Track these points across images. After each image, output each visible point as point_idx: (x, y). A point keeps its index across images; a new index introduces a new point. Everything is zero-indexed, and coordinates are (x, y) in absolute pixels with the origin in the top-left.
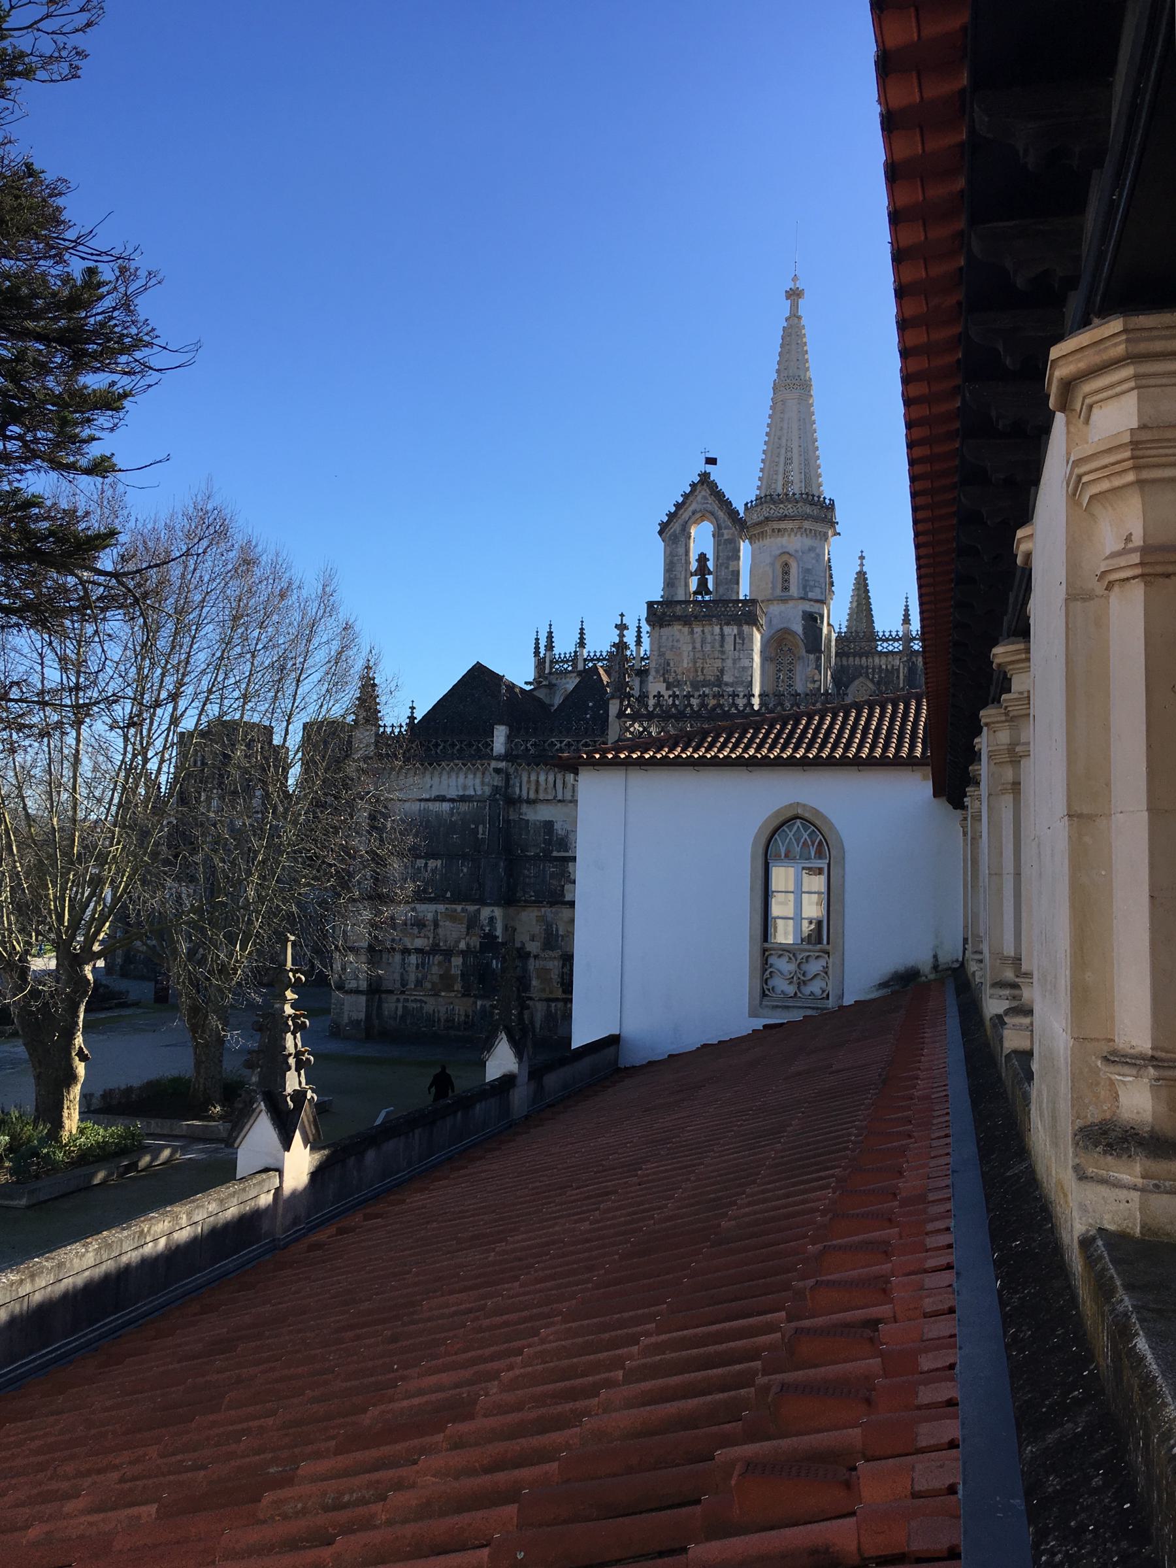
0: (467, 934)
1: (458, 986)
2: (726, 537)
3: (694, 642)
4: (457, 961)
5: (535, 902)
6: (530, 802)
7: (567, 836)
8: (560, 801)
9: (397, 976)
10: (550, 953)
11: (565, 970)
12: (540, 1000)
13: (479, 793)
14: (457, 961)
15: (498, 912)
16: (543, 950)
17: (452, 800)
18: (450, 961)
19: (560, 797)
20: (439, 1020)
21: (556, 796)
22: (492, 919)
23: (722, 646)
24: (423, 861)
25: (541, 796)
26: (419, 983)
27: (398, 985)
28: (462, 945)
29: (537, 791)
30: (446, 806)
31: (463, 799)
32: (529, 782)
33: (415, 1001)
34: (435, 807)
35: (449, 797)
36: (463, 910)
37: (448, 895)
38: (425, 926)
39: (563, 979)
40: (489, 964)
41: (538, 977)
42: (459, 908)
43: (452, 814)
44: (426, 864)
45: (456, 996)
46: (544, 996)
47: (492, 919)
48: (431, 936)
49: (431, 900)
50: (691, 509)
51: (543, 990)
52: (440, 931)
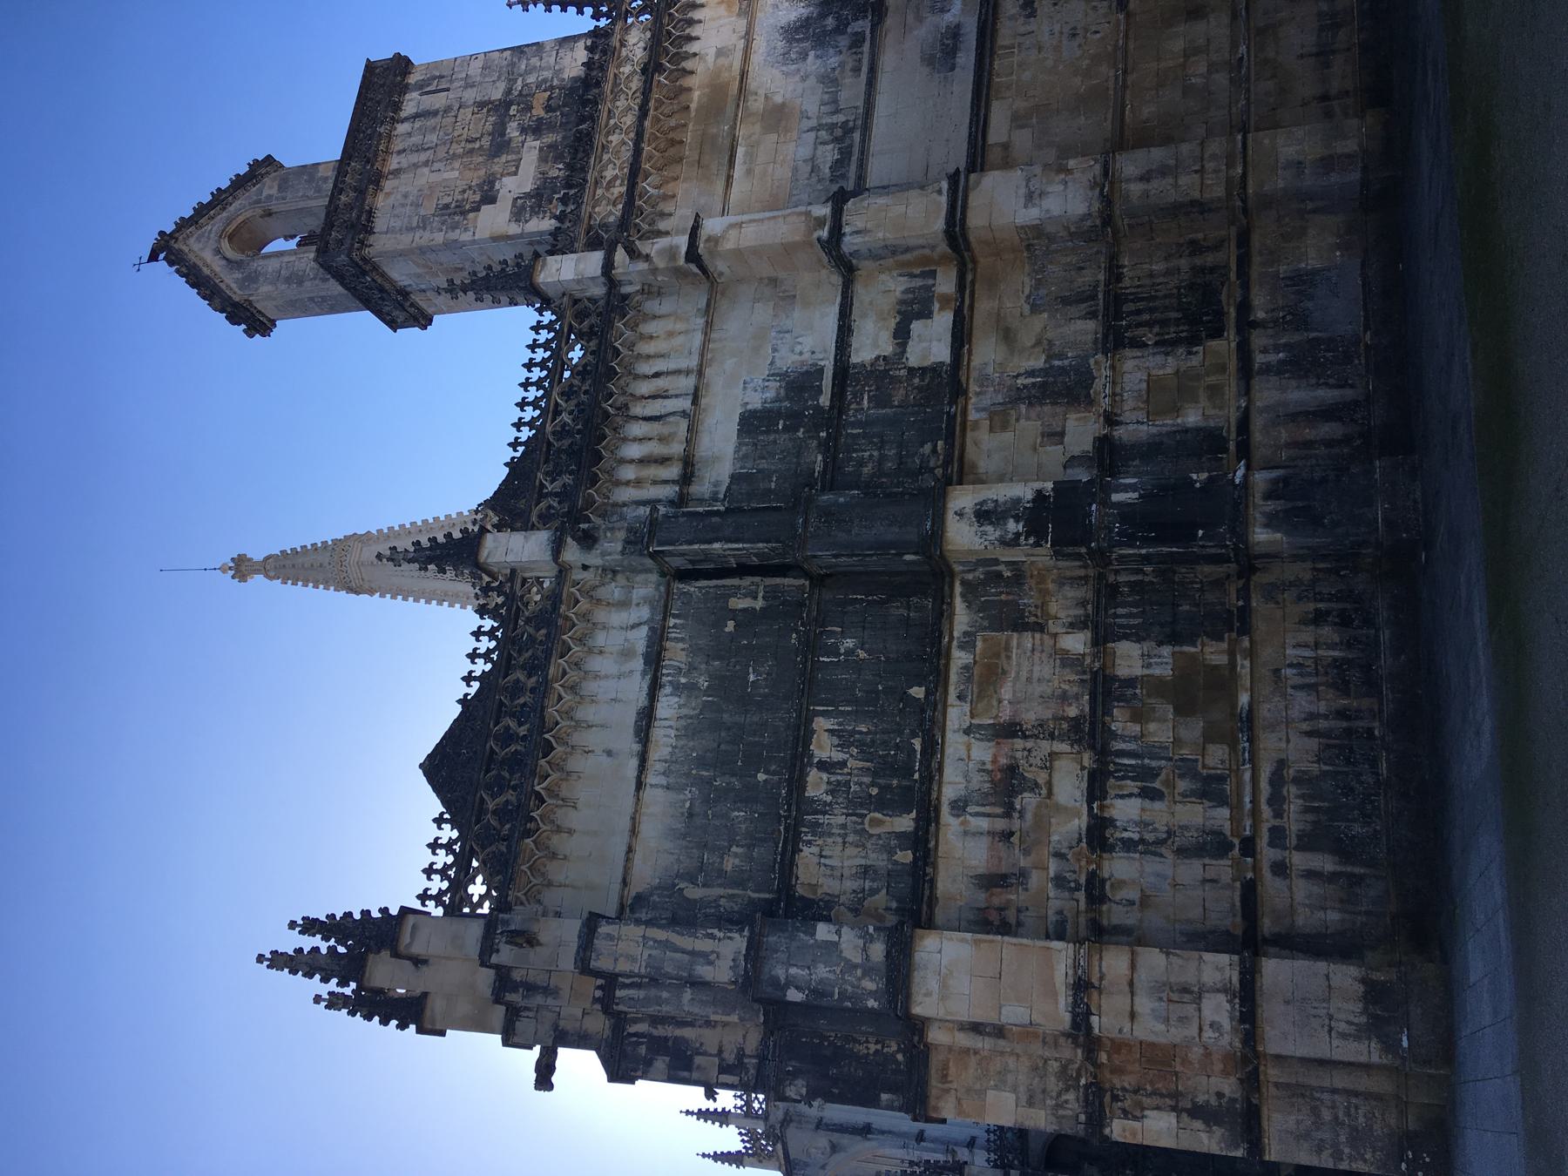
0: (1040, 628)
1: (1214, 653)
2: (274, 191)
3: (416, 166)
4: (1129, 659)
5: (950, 437)
6: (687, 478)
7: (783, 376)
8: (695, 401)
9: (1192, 870)
10: (1098, 385)
11: (1150, 339)
12: (1247, 391)
13: (645, 613)
14: (1129, 659)
15: (963, 499)
16: (1091, 402)
17: (652, 695)
18: (1131, 682)
19: (686, 404)
20: (1341, 714)
21: (684, 414)
22: (984, 515)
23: (435, 113)
24: (813, 775)
25: (677, 448)
26: (1210, 789)
27: (1223, 869)
28: (1076, 643)
29: (663, 461)
30: (667, 707)
31: (654, 659)
32: (638, 483)
33: (1277, 801)
34: (664, 740)
35: (643, 700)
36: (968, 644)
37: (918, 692)
38: (1012, 770)
39: (1175, 343)
40: (1126, 512)
41: (1176, 410)
42: (960, 658)
43: (692, 687)
44: (824, 766)
45: (1251, 654)
46: (1232, 387)
47: (984, 515)
48: (1046, 746)
49: (933, 747)
50: (208, 255)
51: (1214, 391)
52: (1030, 716)
